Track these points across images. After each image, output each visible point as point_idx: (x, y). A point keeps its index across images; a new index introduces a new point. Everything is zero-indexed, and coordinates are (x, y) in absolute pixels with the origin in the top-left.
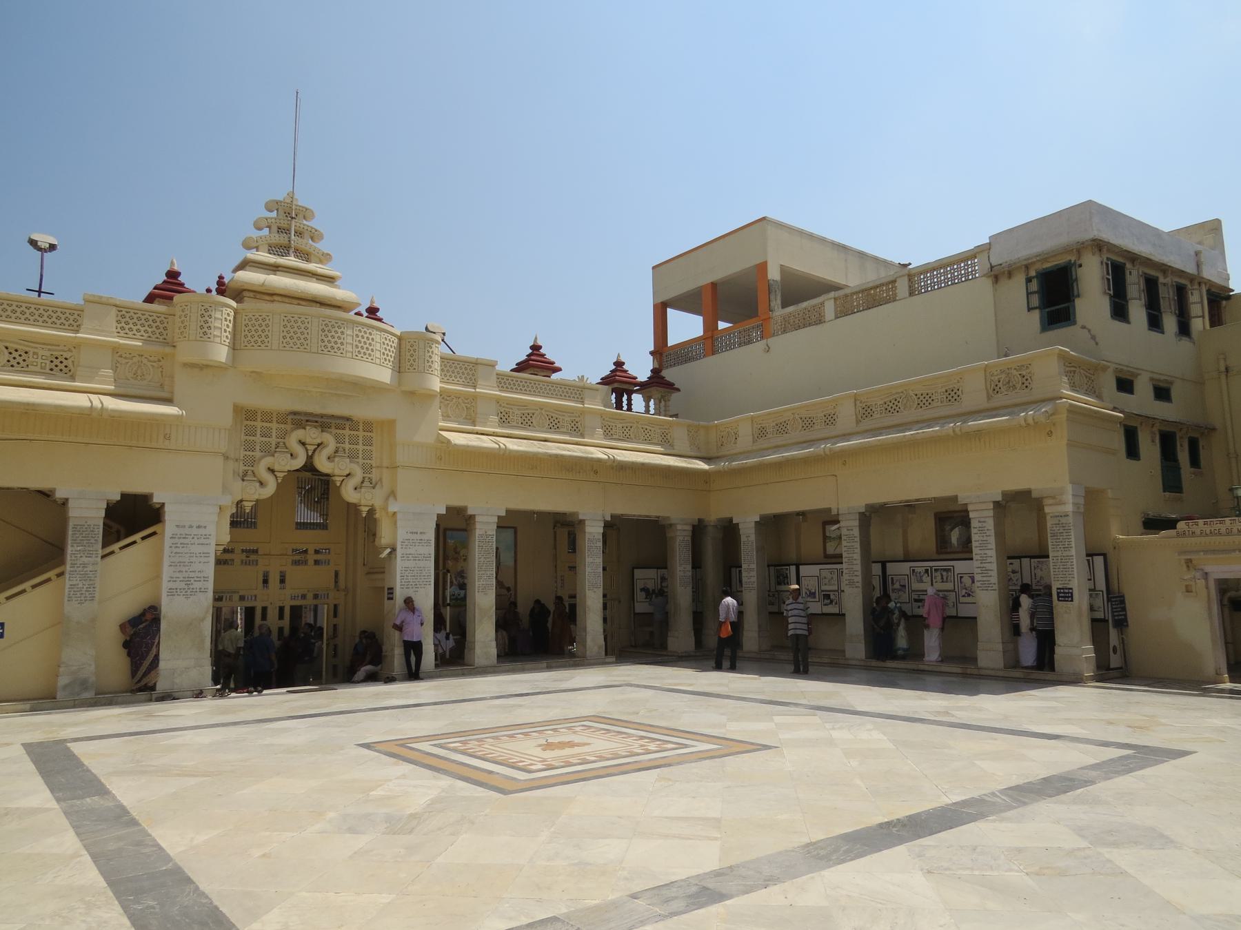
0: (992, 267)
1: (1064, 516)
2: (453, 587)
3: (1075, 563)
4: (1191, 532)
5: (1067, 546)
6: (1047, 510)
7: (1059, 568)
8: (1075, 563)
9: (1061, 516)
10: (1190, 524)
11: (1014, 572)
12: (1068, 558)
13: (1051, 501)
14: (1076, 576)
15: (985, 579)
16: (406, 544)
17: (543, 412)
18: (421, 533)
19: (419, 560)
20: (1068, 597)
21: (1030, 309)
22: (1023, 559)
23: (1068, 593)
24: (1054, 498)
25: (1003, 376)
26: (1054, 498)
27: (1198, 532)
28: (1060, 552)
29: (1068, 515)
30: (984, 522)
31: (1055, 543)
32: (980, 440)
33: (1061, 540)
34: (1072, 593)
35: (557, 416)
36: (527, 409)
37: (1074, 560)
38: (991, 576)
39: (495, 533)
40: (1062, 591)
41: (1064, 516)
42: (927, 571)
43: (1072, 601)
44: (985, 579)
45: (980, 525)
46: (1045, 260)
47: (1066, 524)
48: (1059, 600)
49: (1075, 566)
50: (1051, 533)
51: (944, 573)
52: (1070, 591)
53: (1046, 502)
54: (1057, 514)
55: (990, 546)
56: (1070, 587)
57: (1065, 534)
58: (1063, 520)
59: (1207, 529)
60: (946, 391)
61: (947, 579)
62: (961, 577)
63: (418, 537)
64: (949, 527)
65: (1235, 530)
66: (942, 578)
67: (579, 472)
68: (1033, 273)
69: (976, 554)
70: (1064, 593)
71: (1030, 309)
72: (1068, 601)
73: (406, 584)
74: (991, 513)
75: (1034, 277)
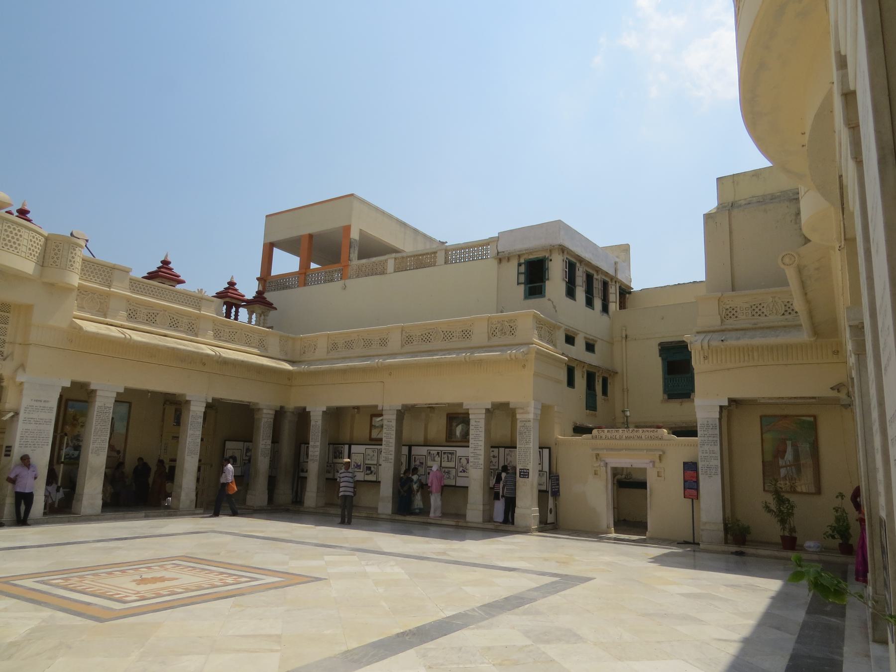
0: (498, 253)
1: (528, 421)
2: (69, 448)
3: (532, 452)
6: (518, 416)
8: (532, 452)
10: (600, 431)
11: (494, 457)
13: (521, 411)
15: (476, 461)
16: (30, 409)
17: (166, 313)
18: (45, 401)
19: (39, 424)
21: (518, 284)
22: (500, 449)
23: (526, 472)
24: (522, 408)
25: (499, 325)
26: (522, 408)
27: (604, 437)
29: (530, 421)
30: (479, 422)
32: (481, 366)
34: (528, 473)
35: (178, 318)
36: (153, 309)
37: (532, 451)
38: (480, 459)
39: (112, 406)
40: (523, 471)
42: (438, 453)
43: (528, 478)
44: (476, 461)
45: (476, 424)
46: (531, 253)
48: (520, 477)
49: (532, 455)
51: (450, 456)
53: (518, 411)
54: (523, 420)
55: (481, 439)
56: (526, 468)
57: (527, 433)
58: (527, 424)
59: (609, 435)
60: (463, 331)
61: (451, 459)
62: (460, 459)
63: (43, 404)
64: (456, 424)
65: (624, 437)
66: (448, 459)
67: (191, 363)
68: (522, 261)
69: (471, 444)
70: (524, 472)
71: (518, 284)
72: (526, 478)
73: (25, 443)
74: (484, 416)
75: (523, 263)
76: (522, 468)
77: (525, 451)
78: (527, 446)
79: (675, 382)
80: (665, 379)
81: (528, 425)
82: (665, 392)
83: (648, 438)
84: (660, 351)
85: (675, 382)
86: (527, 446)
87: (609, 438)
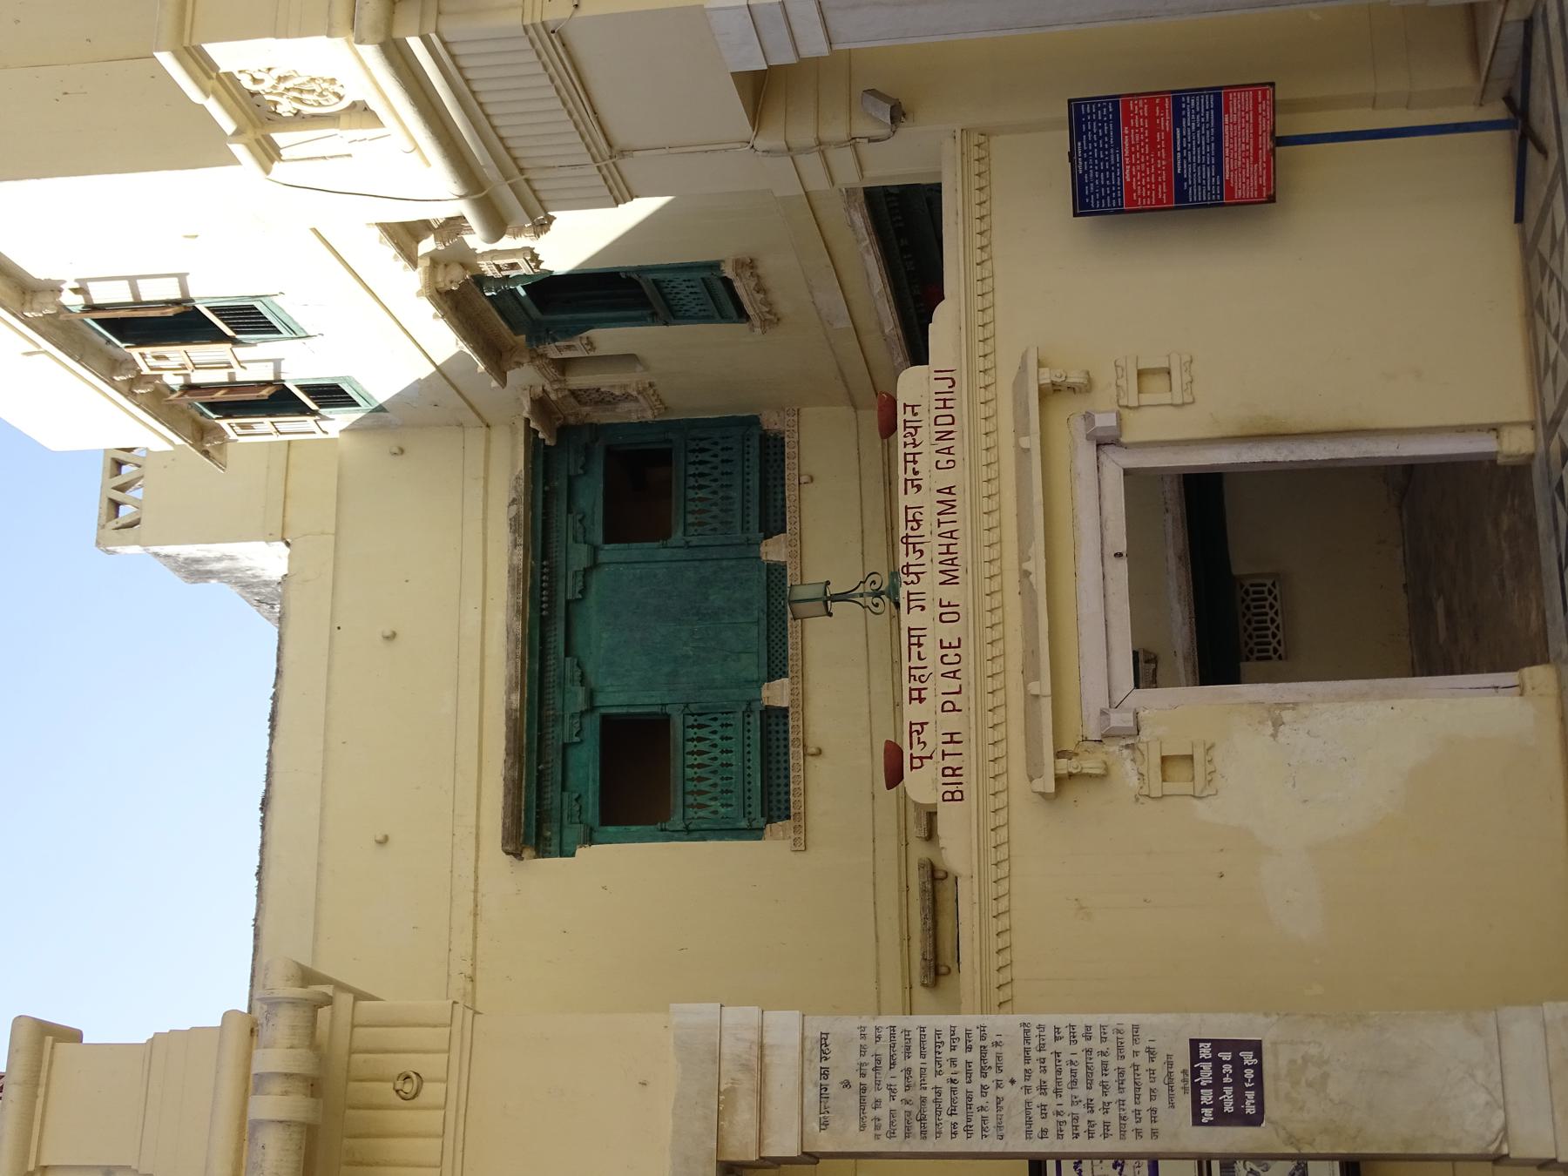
1: (824, 1056)
3: (1062, 1020)
4: (949, 748)
5: (974, 1056)
7: (1090, 1106)
9: (825, 1073)
12: (1034, 1054)
13: (743, 1116)
14: (1128, 1020)
20: (1238, 1064)
23: (1217, 1064)
26: (724, 1102)
28: (1008, 1091)
29: (824, 1040)
31: (960, 1119)
33: (941, 1081)
34: (1218, 1045)
40: (1207, 1096)
41: (824, 1056)
43: (1256, 1047)
47: (863, 1051)
48: (1256, 1120)
49: (1080, 1020)
50: (907, 1135)
52: (1205, 1051)
54: (812, 1093)
56: (1183, 1062)
57: (915, 1062)
58: (844, 1063)
59: (936, 688)
70: (1217, 1085)
72: (1258, 1069)
76: (1185, 1102)
77: (1050, 1077)
78: (1014, 1066)
79: (703, 786)
80: (690, 832)
81: (854, 1058)
82: (754, 833)
83: (949, 450)
84: (541, 852)
85: (703, 786)
86: (1014, 1066)
87: (953, 685)
